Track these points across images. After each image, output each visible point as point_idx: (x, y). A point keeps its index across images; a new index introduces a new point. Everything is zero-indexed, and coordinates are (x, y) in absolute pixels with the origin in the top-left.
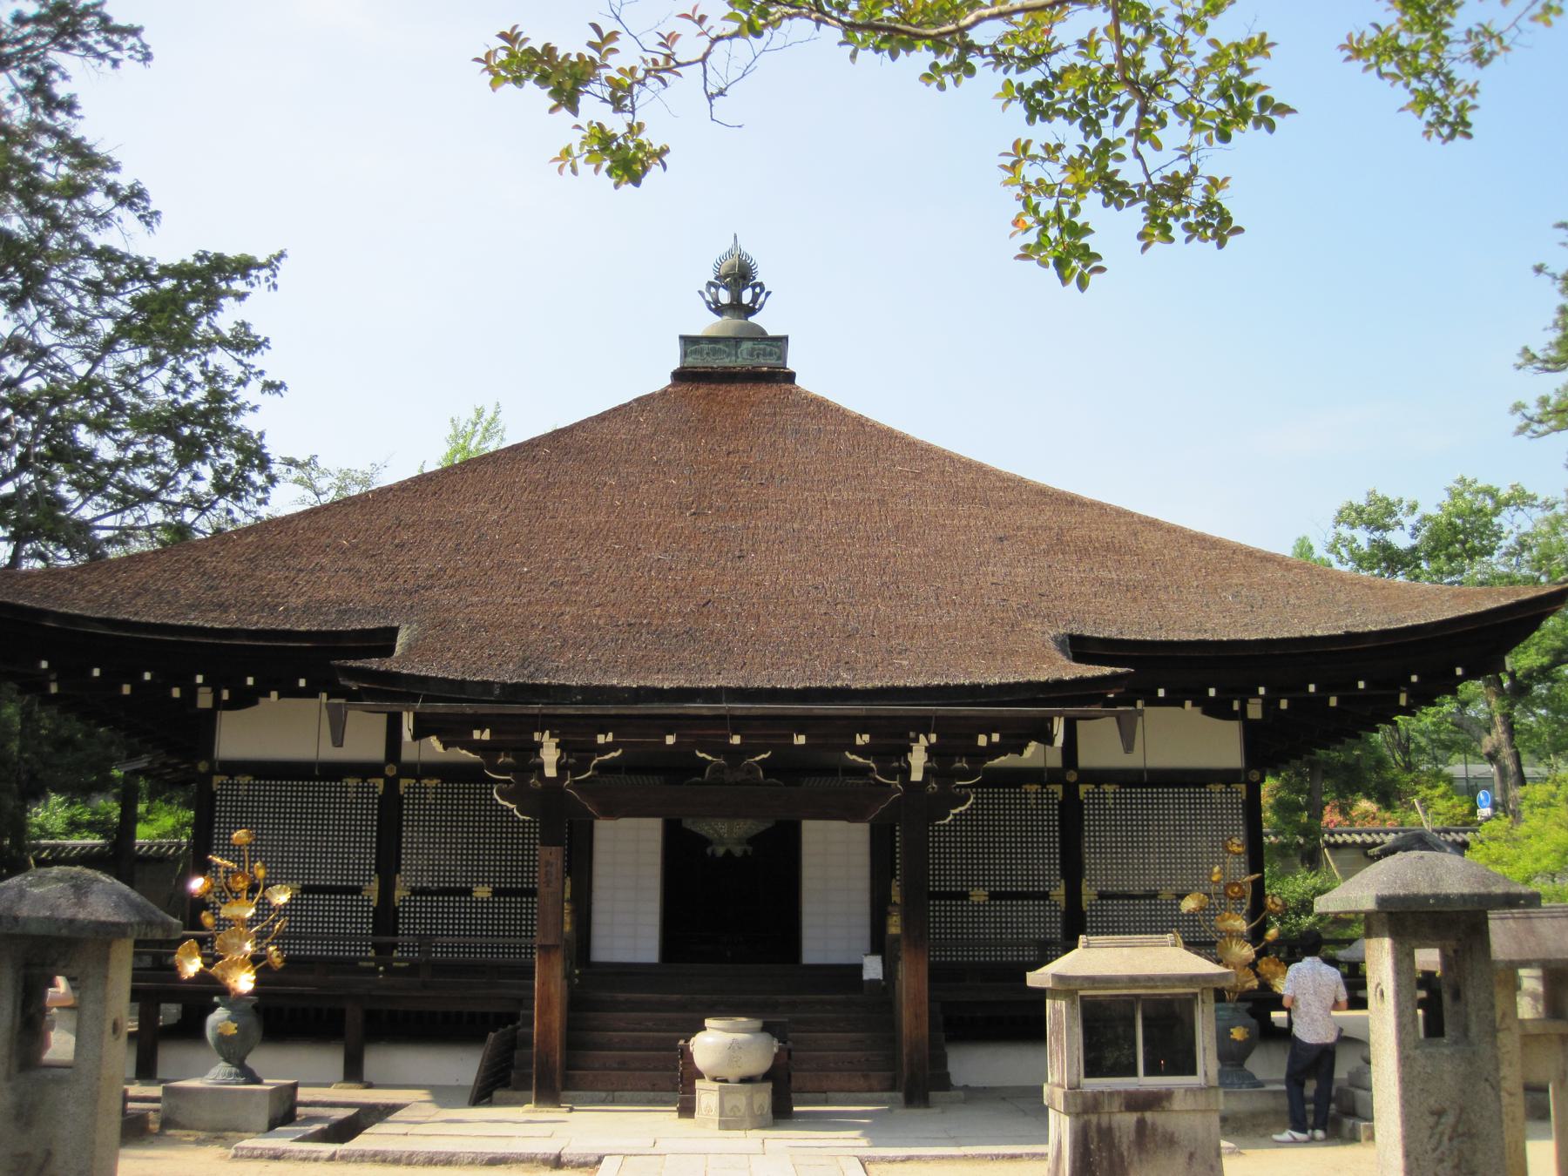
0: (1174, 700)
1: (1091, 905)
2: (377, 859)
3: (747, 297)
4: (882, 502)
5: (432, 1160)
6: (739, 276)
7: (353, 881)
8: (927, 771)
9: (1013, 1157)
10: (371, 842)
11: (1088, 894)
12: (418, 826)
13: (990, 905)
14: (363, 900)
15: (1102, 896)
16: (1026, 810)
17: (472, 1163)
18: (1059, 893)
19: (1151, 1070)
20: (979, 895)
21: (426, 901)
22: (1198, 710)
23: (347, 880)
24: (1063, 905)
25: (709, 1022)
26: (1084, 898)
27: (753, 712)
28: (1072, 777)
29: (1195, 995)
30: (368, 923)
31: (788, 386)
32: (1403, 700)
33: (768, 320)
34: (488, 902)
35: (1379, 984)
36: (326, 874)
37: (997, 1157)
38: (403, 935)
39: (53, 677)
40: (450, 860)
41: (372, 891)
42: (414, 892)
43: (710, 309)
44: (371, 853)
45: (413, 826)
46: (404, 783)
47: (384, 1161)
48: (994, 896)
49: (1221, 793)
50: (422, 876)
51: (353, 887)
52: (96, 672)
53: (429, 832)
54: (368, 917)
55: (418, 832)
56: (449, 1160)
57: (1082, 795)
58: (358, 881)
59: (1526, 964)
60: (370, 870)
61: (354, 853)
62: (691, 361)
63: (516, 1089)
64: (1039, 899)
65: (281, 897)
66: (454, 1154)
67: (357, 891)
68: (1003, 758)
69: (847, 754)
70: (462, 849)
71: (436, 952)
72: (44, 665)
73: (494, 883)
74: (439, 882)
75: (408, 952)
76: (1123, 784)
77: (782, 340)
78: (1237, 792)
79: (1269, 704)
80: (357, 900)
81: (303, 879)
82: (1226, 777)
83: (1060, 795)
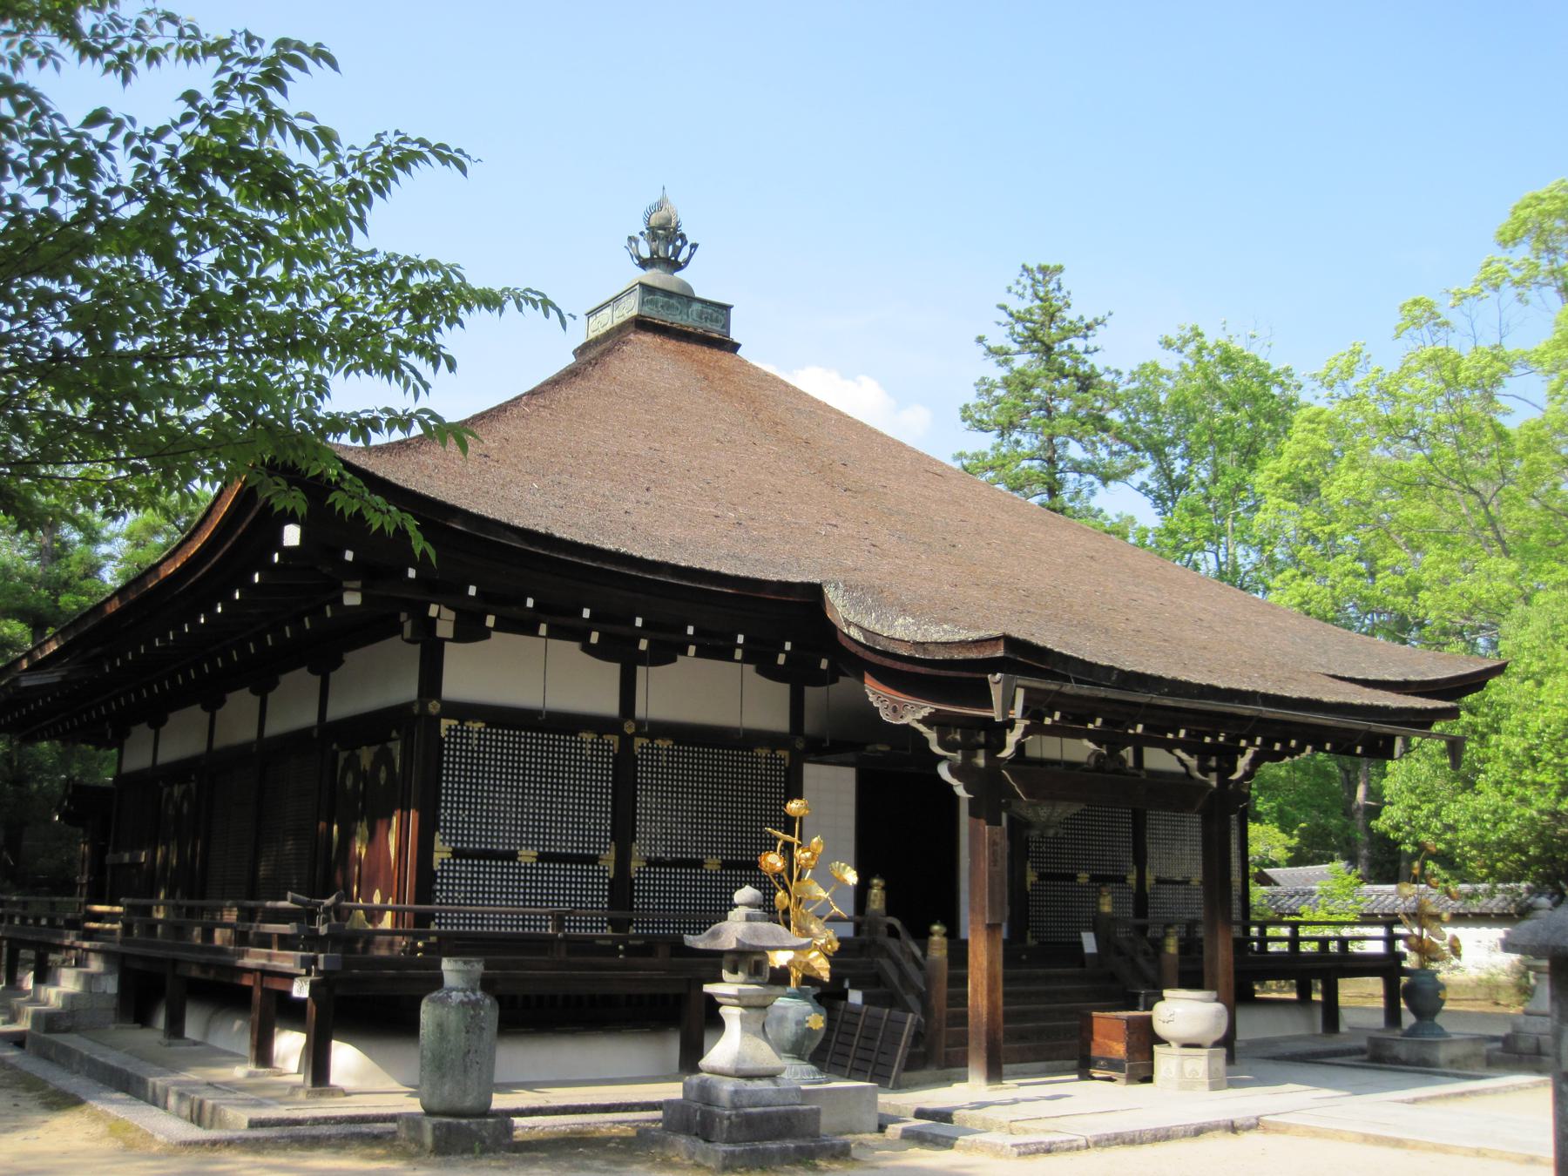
1: (639, 872)
2: (612, 825)
5: (1315, 1133)
7: (589, 849)
9: (1462, 1094)
10: (607, 806)
11: (1150, 879)
12: (652, 790)
13: (721, 875)
14: (599, 871)
17: (1184, 1136)
18: (1132, 879)
20: (1083, 878)
21: (670, 873)
23: (583, 848)
25: (1166, 993)
30: (603, 896)
34: (531, 868)
36: (561, 840)
37: (1448, 1096)
38: (638, 909)
40: (682, 829)
42: (651, 862)
44: (606, 819)
45: (646, 790)
46: (638, 742)
47: (1124, 1143)
54: (604, 890)
55: (651, 797)
56: (1162, 1136)
58: (594, 849)
60: (606, 837)
61: (590, 818)
62: (647, 311)
63: (941, 1067)
66: (1168, 1130)
67: (594, 860)
70: (692, 817)
71: (569, 927)
73: (538, 846)
74: (671, 852)
75: (643, 928)
77: (725, 309)
80: (593, 871)
81: (722, 854)
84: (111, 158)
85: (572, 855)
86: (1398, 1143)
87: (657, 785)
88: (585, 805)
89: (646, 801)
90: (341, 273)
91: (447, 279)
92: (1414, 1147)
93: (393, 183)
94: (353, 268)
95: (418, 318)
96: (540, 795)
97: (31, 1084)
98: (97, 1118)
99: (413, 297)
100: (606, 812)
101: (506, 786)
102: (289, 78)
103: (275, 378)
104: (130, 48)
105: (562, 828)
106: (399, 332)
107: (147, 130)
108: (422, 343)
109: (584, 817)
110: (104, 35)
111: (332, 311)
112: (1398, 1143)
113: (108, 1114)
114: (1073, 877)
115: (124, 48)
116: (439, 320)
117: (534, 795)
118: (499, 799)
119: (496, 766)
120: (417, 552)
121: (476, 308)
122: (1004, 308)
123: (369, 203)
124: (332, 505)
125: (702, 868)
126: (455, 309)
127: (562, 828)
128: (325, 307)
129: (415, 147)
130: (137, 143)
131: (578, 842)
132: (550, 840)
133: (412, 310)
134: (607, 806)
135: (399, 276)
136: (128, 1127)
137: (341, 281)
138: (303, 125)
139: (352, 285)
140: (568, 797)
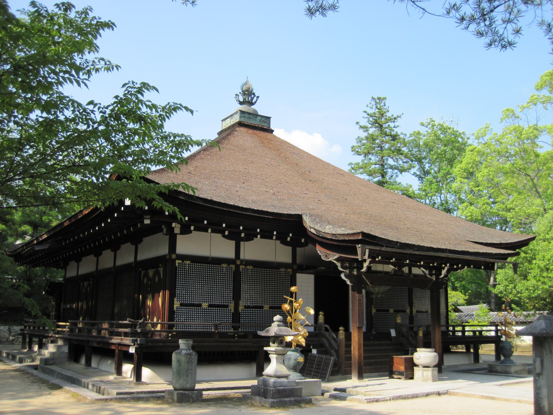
1: (242, 310)
2: (233, 295)
7: (225, 303)
9: (518, 383)
10: (231, 288)
11: (414, 311)
12: (246, 283)
13: (269, 311)
14: (229, 310)
15: (417, 312)
17: (423, 396)
18: (408, 311)
20: (391, 311)
23: (223, 303)
25: (418, 349)
30: (230, 319)
31: (270, 134)
34: (206, 309)
36: (216, 300)
37: (512, 383)
40: (256, 296)
42: (246, 307)
44: (231, 293)
45: (244, 283)
46: (241, 267)
47: (402, 398)
50: (247, 301)
51: (225, 305)
54: (230, 316)
55: (246, 285)
58: (227, 303)
60: (231, 299)
61: (225, 292)
62: (242, 119)
63: (343, 375)
66: (417, 394)
67: (227, 306)
70: (259, 292)
73: (209, 302)
75: (243, 329)
77: (269, 118)
80: (227, 310)
84: (94, 114)
85: (220, 305)
86: (493, 398)
87: (248, 281)
88: (224, 288)
89: (244, 287)
90: (155, 138)
91: (186, 138)
92: (498, 400)
93: (172, 115)
94: (159, 136)
95: (177, 149)
96: (209, 285)
97: (44, 382)
98: (67, 392)
99: (176, 144)
100: (231, 290)
101: (198, 282)
102: (144, 92)
103: (135, 168)
104: (90, 68)
105: (216, 296)
106: (172, 154)
107: (104, 106)
108: (178, 156)
109: (224, 292)
110: (83, 65)
111: (152, 149)
112: (493, 398)
113: (71, 391)
114: (388, 311)
115: (89, 68)
116: (183, 150)
117: (207, 285)
118: (195, 286)
119: (194, 276)
120: (179, 218)
121: (194, 145)
122: (365, 112)
123: (165, 121)
124: (153, 205)
125: (263, 309)
126: (188, 146)
127: (216, 296)
128: (151, 147)
129: (179, 106)
130: (101, 109)
131: (222, 300)
132: (212, 300)
133: (176, 147)
134: (231, 288)
135: (172, 138)
136: (78, 395)
137: (155, 140)
138: (148, 103)
139: (159, 141)
140: (218, 286)
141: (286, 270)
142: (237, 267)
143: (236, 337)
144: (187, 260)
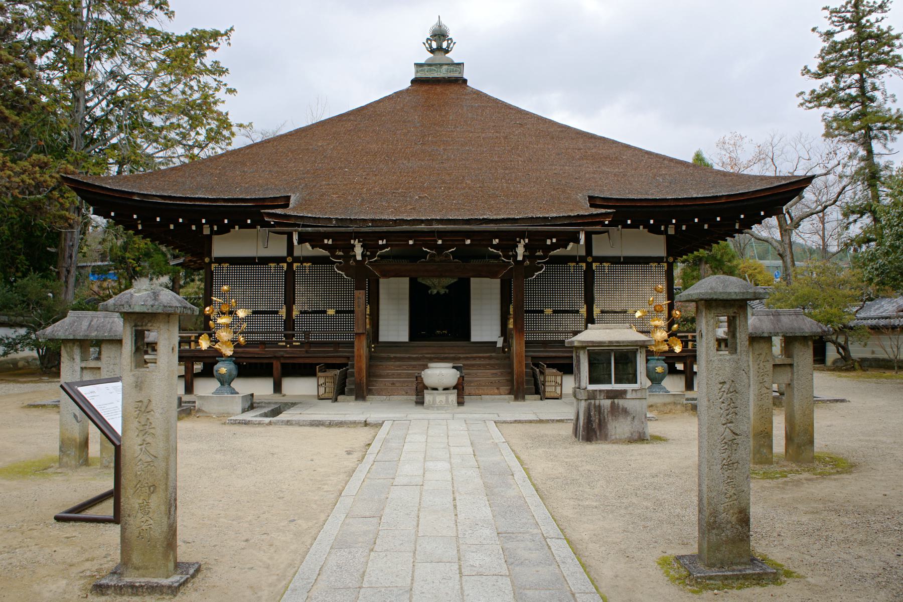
0: (634, 226)
2: (285, 299)
3: (445, 45)
4: (506, 138)
6: (440, 35)
8: (524, 256)
11: (596, 311)
15: (602, 312)
16: (569, 274)
19: (617, 382)
20: (548, 311)
22: (646, 230)
24: (585, 315)
26: (594, 312)
27: (447, 230)
28: (590, 259)
29: (637, 349)
30: (282, 326)
32: (737, 227)
33: (454, 56)
34: (334, 316)
35: (701, 331)
39: (139, 222)
40: (317, 298)
41: (283, 312)
42: (301, 312)
43: (428, 51)
45: (300, 284)
46: (295, 265)
48: (555, 312)
49: (656, 267)
50: (305, 306)
51: (274, 311)
52: (158, 219)
53: (307, 286)
57: (594, 268)
59: (776, 334)
62: (419, 75)
64: (575, 313)
65: (241, 313)
67: (277, 312)
68: (558, 250)
69: (489, 248)
71: (312, 338)
72: (135, 216)
73: (336, 308)
74: (312, 308)
76: (612, 263)
78: (663, 267)
79: (678, 227)
82: (659, 260)
83: (584, 268)
87: (305, 281)
114: (542, 312)
141: (278, 265)
142: (589, 265)
143: (287, 348)
144: (225, 263)
